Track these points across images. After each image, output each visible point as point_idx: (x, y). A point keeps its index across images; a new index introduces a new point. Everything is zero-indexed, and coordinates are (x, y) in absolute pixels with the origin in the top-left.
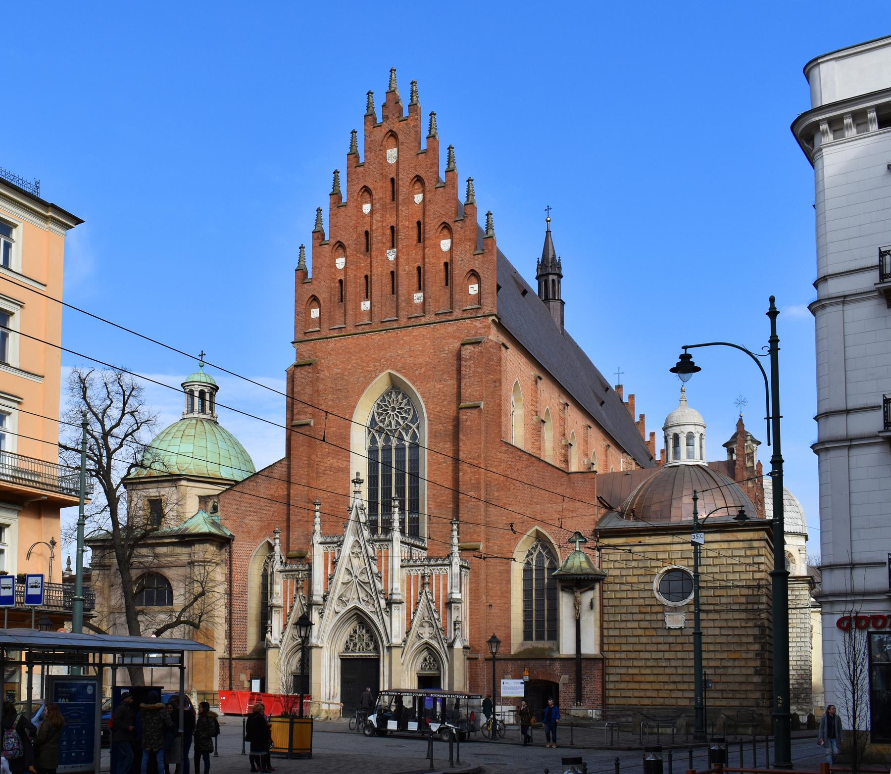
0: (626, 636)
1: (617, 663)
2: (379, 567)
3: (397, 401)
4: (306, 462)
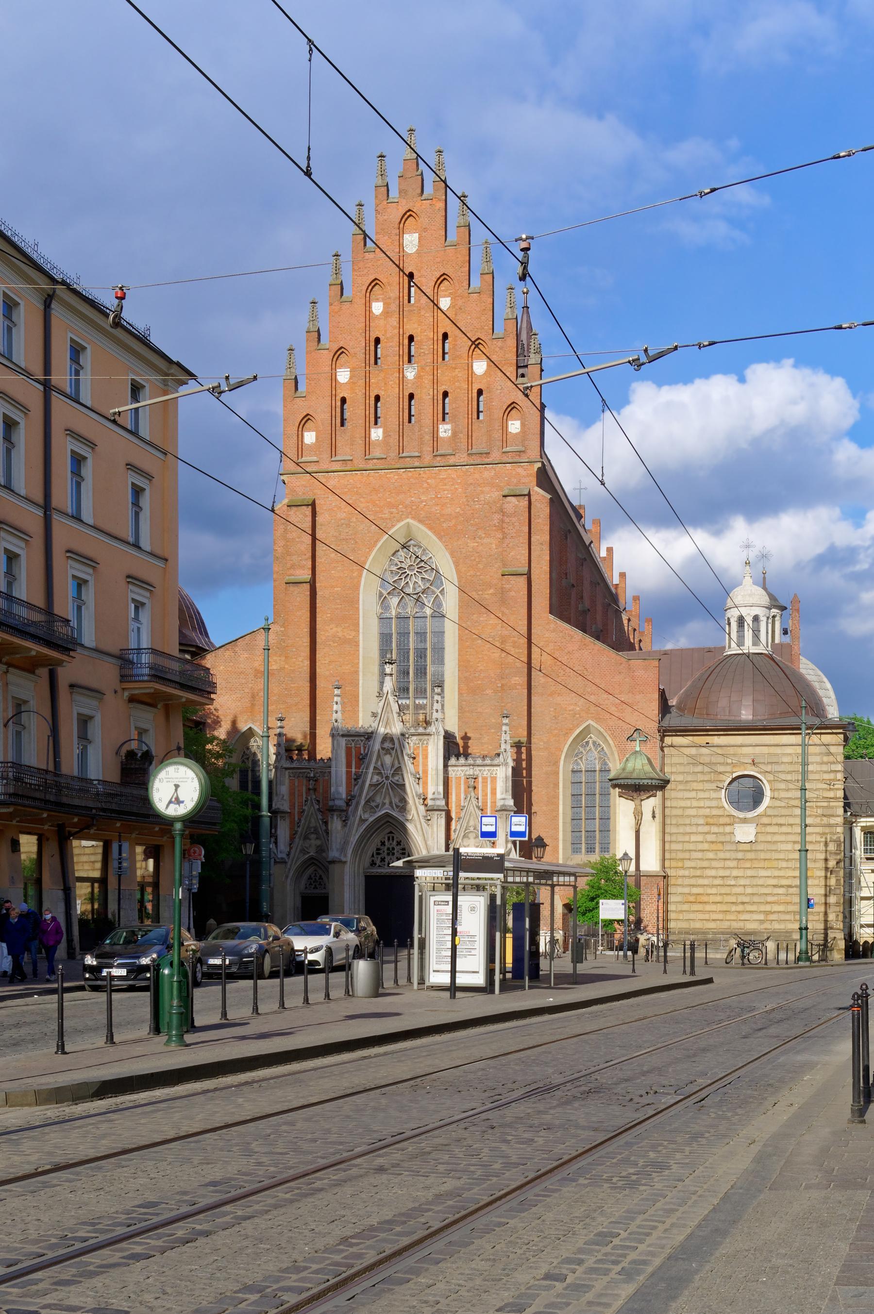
0: (690, 851)
1: (680, 881)
4: (306, 630)
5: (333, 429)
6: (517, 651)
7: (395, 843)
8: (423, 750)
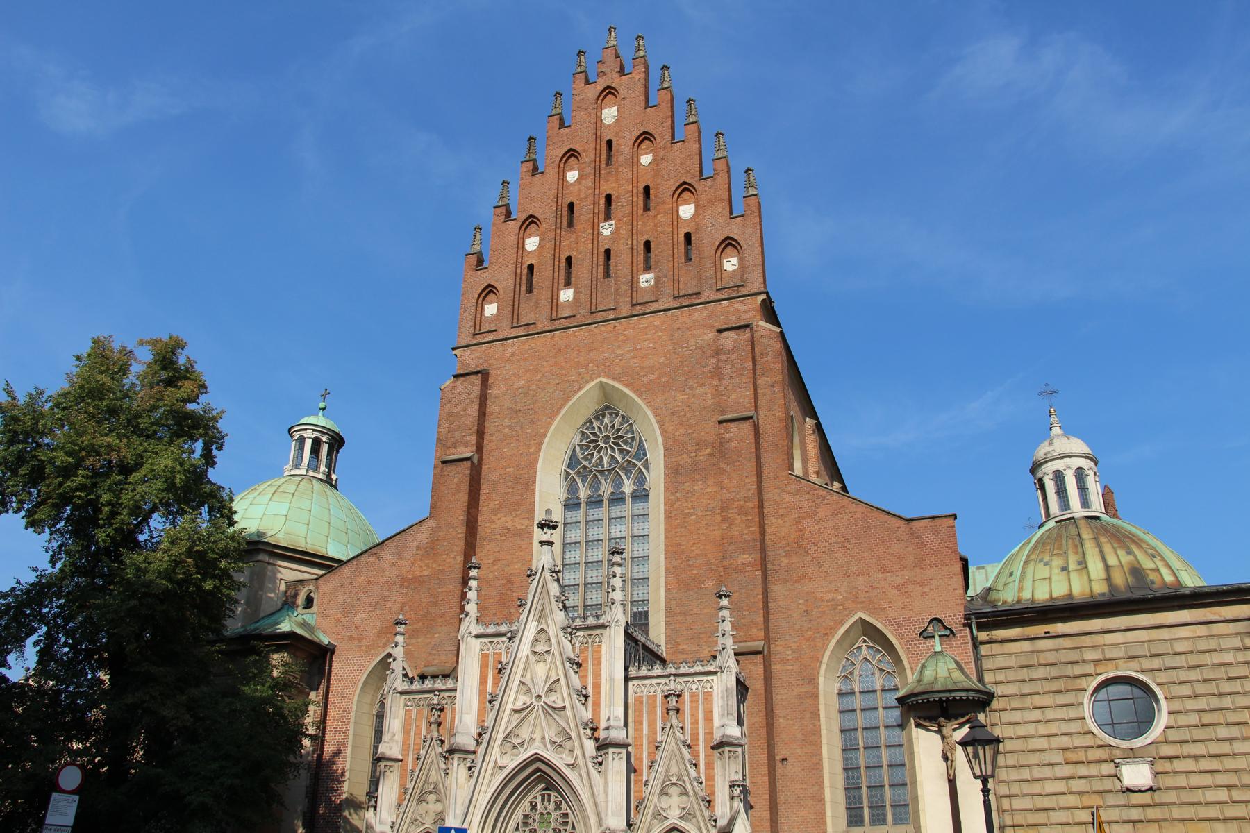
2: (583, 678)
3: (613, 426)
4: (462, 518)
5: (517, 296)
6: (744, 518)
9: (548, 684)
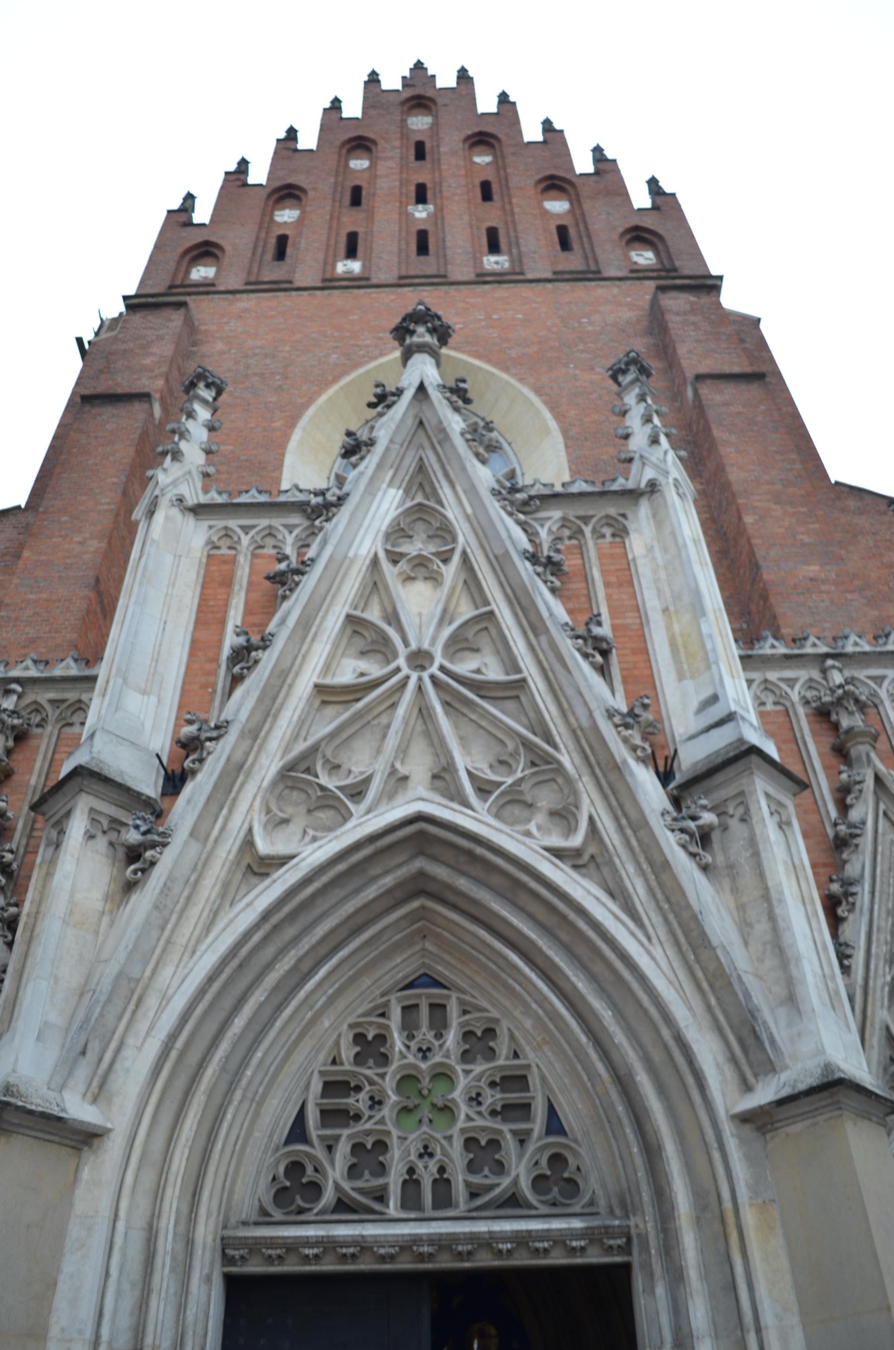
4: (115, 480)
6: (790, 509)
7: (452, 1038)
8: (601, 556)
9: (447, 631)
